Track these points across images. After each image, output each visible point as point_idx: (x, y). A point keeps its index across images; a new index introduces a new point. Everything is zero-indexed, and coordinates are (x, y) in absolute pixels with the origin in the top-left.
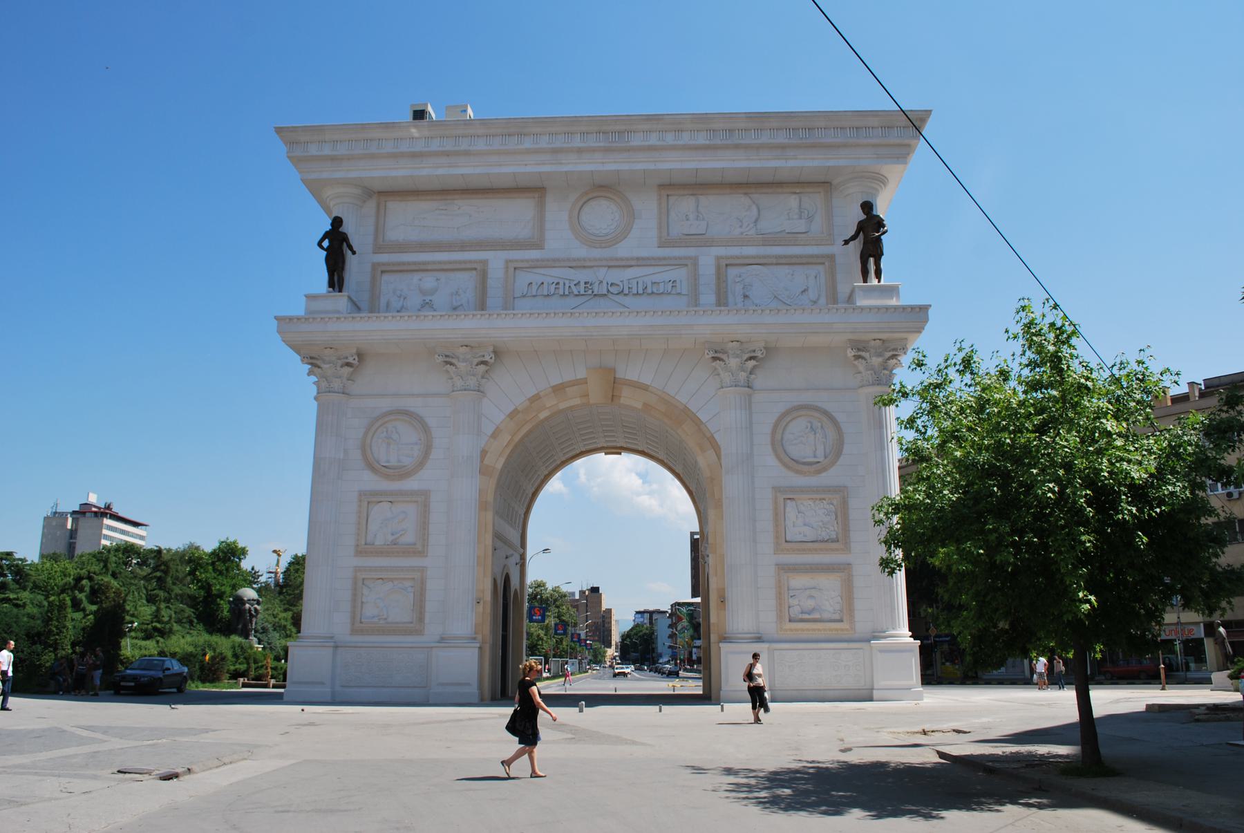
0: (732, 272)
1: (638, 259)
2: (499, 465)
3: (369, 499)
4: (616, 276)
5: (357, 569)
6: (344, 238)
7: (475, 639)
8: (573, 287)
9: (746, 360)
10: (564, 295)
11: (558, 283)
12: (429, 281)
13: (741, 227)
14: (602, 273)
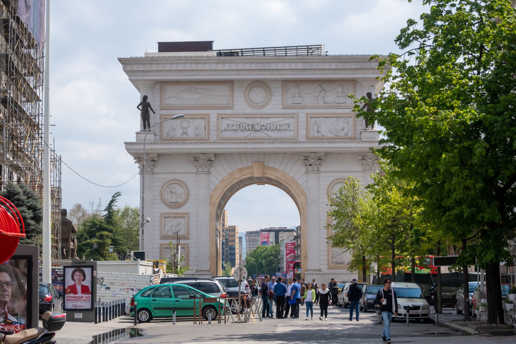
0: (313, 120)
1: (273, 114)
2: (217, 202)
3: (166, 216)
4: (264, 122)
5: (161, 245)
6: (149, 105)
7: (210, 271)
8: (246, 127)
9: (317, 160)
10: (243, 130)
11: (240, 125)
12: (185, 124)
13: (317, 100)
14: (258, 120)
